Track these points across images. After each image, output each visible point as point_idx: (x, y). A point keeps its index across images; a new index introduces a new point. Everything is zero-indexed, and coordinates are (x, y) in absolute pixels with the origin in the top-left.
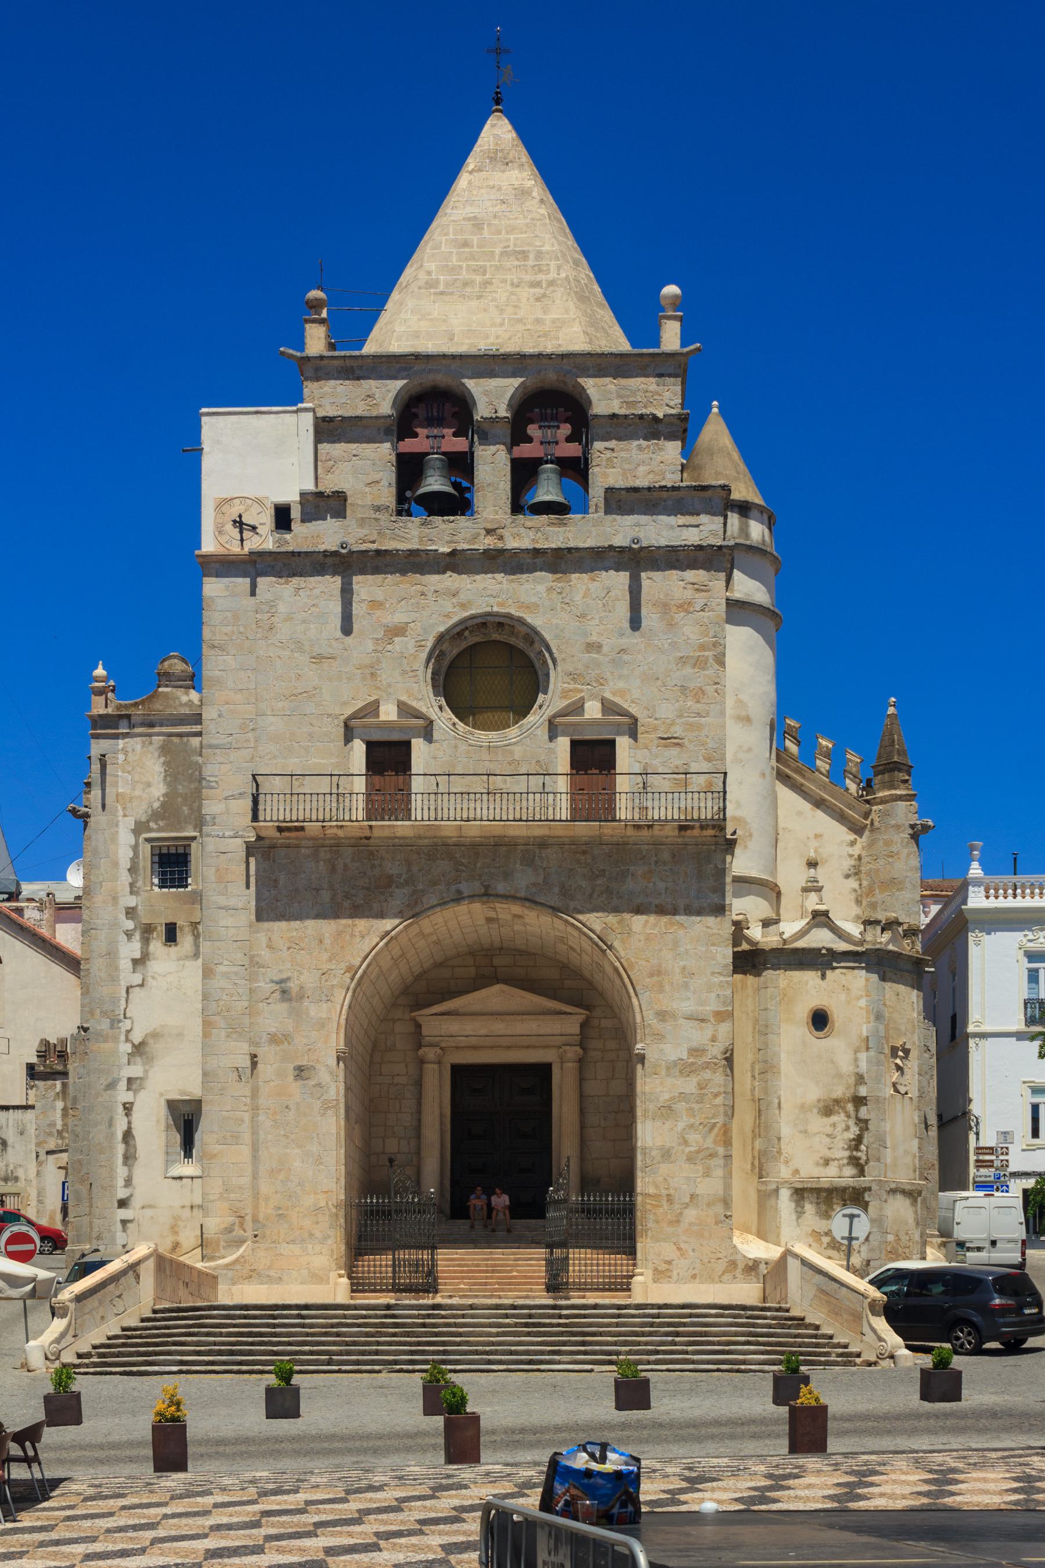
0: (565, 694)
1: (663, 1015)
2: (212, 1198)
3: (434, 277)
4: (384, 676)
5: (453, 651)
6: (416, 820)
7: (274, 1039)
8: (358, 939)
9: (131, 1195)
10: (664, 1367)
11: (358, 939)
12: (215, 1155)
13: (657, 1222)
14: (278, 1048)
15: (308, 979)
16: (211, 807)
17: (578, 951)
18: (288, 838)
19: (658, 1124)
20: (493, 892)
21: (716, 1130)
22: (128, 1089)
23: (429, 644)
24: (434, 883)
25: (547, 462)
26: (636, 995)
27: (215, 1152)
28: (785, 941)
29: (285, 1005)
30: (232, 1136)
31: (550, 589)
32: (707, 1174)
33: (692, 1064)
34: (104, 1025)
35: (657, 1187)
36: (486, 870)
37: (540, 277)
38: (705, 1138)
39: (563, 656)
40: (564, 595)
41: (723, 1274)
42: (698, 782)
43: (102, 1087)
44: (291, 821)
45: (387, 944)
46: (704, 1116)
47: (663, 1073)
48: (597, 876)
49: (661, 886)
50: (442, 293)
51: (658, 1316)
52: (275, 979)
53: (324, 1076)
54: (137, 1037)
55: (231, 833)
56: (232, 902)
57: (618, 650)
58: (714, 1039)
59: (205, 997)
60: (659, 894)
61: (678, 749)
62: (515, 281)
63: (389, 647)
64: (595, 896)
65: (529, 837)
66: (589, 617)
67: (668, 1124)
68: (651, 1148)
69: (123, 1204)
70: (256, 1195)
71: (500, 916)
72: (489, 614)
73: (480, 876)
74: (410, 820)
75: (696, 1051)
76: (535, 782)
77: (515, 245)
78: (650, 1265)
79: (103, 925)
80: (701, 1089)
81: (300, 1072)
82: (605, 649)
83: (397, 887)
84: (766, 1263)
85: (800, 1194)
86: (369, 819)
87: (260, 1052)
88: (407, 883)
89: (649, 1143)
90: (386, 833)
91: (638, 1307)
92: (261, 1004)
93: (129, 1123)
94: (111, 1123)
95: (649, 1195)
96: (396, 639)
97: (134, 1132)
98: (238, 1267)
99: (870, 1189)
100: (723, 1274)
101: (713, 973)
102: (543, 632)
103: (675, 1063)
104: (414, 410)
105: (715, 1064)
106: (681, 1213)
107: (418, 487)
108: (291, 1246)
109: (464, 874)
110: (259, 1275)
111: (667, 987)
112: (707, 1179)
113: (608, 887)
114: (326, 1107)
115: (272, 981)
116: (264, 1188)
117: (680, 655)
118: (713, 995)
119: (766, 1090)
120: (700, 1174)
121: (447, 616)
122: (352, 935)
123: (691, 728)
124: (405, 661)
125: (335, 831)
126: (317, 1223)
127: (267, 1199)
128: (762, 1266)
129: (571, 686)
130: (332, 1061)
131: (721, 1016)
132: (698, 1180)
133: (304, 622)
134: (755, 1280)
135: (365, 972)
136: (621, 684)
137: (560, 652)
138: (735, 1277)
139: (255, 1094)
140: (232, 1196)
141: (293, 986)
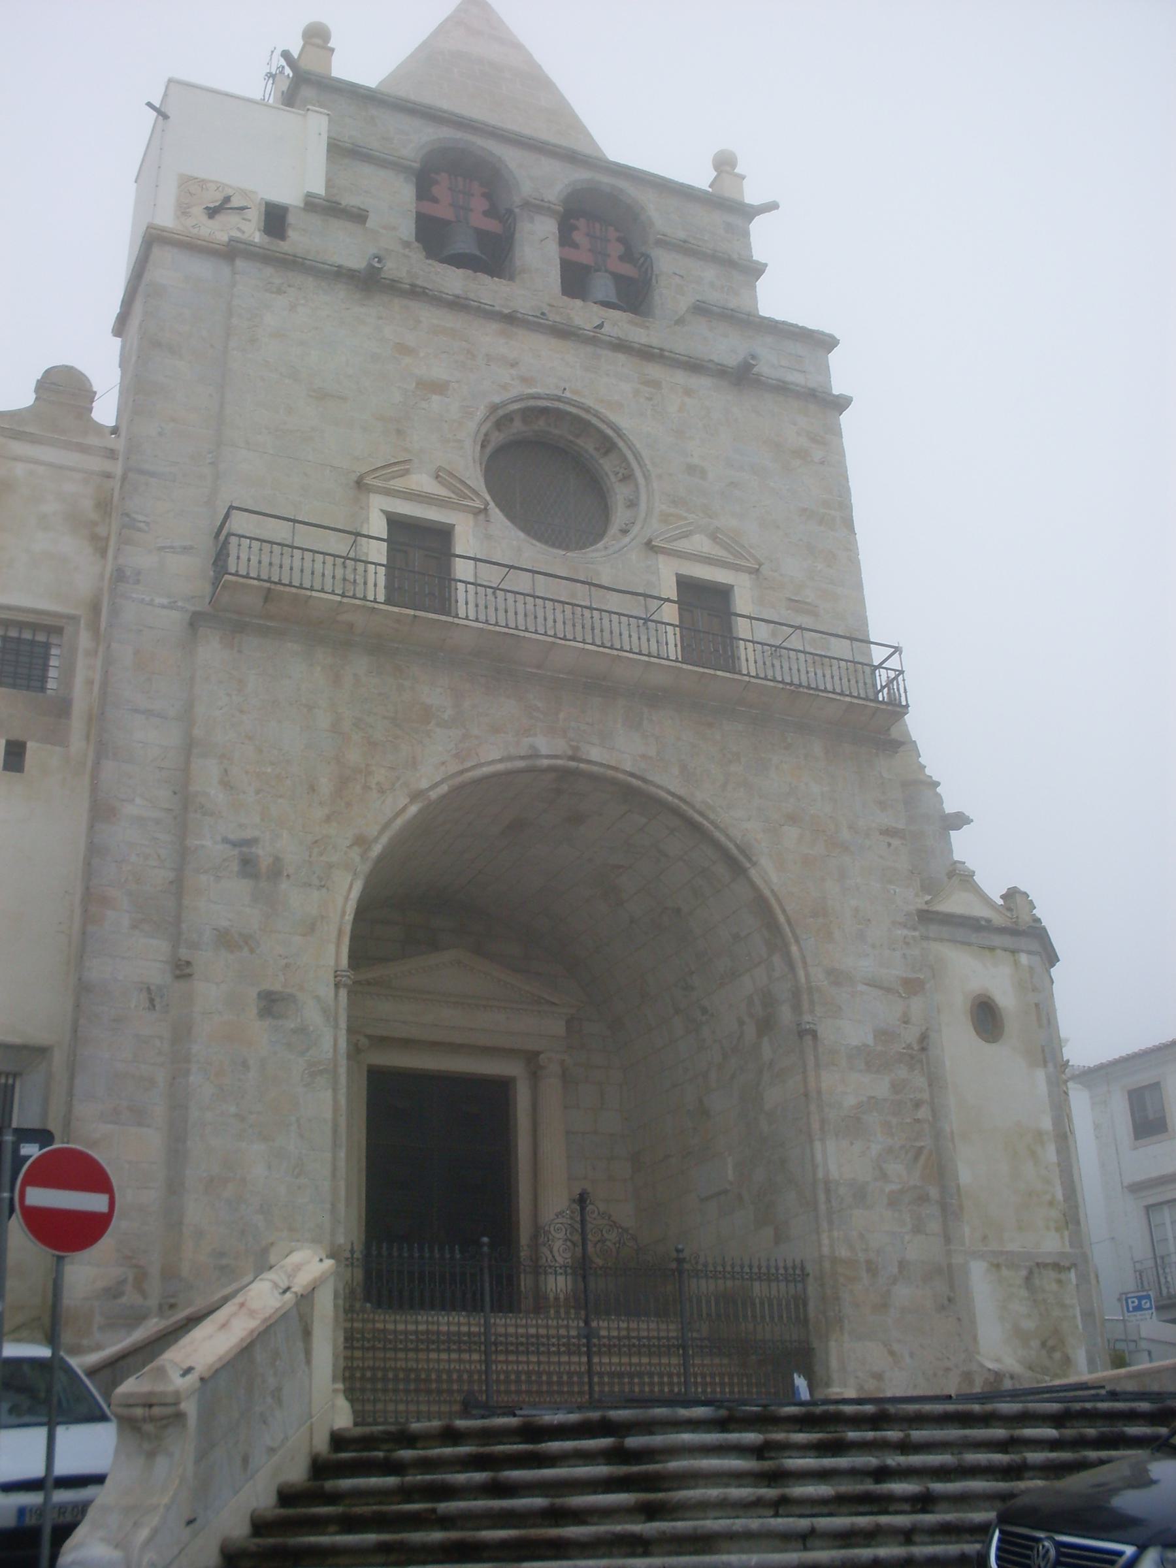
1: (837, 977)
5: (498, 438)
7: (226, 940)
21: (923, 1158)
26: (797, 941)
32: (918, 1229)
52: (232, 837)
55: (165, 601)
58: (906, 1021)
72: (559, 399)
75: (884, 1035)
89: (834, 1173)
96: (435, 398)
115: (225, 840)
121: (505, 387)
122: (366, 788)
130: (326, 991)
132: (907, 1238)
139: (182, 1033)
141: (264, 853)
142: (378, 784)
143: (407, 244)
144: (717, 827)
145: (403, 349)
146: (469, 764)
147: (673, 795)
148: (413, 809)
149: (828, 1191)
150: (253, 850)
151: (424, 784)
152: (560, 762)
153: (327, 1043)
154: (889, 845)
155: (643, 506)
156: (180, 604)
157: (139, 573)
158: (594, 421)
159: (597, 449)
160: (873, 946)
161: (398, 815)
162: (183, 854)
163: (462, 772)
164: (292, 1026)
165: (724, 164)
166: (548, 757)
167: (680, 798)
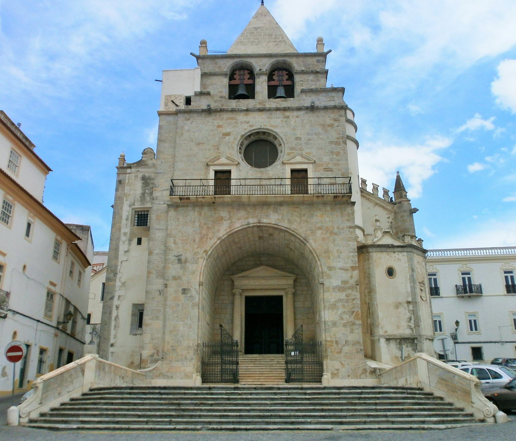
0: (288, 154)
1: (330, 268)
2: (146, 342)
3: (242, 40)
4: (222, 149)
5: (246, 143)
6: (232, 195)
7: (175, 278)
8: (209, 240)
9: (116, 342)
10: (377, 426)
11: (209, 240)
12: (148, 325)
13: (332, 352)
14: (176, 282)
15: (189, 255)
16: (156, 194)
17: (293, 248)
18: (184, 203)
19: (331, 311)
20: (262, 222)
21: (354, 314)
22: (118, 300)
23: (239, 138)
24: (239, 219)
25: (280, 86)
26: (319, 260)
27: (149, 323)
28: (374, 243)
29: (179, 265)
30: (156, 317)
31: (282, 121)
32: (352, 332)
33: (343, 287)
34: (111, 275)
35: (331, 337)
36: (259, 214)
37: (276, 40)
38: (350, 317)
39: (287, 141)
40: (287, 122)
41: (361, 375)
42: (340, 181)
43: (109, 299)
44: (185, 196)
45: (220, 242)
46: (349, 308)
47: (332, 291)
48: (302, 216)
49: (327, 219)
50: (245, 44)
51: (361, 393)
52: (176, 255)
53: (193, 293)
54: (123, 280)
55: (163, 203)
56: (161, 228)
57: (307, 139)
58: (351, 277)
59: (149, 262)
60: (327, 222)
61: (331, 172)
62: (268, 41)
63: (224, 140)
64: (302, 223)
65: (275, 202)
66: (296, 129)
67: (335, 311)
68: (328, 322)
69: (112, 345)
70: (164, 341)
71: (265, 235)
72: (260, 129)
73: (257, 217)
74: (229, 194)
75: (345, 282)
76: (278, 182)
77: (268, 33)
78: (330, 371)
79: (115, 239)
80: (347, 297)
81: (185, 291)
82: (302, 139)
83: (225, 221)
84: (379, 370)
85: (388, 340)
86: (215, 195)
87: (169, 283)
88: (229, 219)
89: (327, 319)
90: (221, 200)
91: (325, 388)
92: (170, 265)
93: (118, 313)
94: (110, 313)
95: (328, 341)
97: (120, 317)
98: (155, 372)
99: (417, 338)
100: (361, 375)
101: (349, 252)
102: (280, 134)
103: (336, 287)
104: (234, 72)
105: (353, 287)
106: (342, 349)
107: (236, 93)
108: (177, 363)
109: (250, 216)
110: (164, 375)
111: (331, 257)
112: (352, 334)
113: (306, 220)
114: (194, 305)
115: (175, 256)
116: (168, 338)
117: (330, 140)
118: (350, 260)
119: (371, 299)
120: (349, 331)
121: (245, 130)
122: (207, 239)
123: (336, 165)
124: (230, 144)
125: (201, 199)
126: (189, 353)
127: (168, 343)
128: (378, 371)
129: (291, 151)
130: (197, 287)
131: (353, 268)
132: (348, 334)
133: (194, 132)
134: (375, 377)
135: (211, 253)
136: (309, 151)
137: (286, 140)
138: (366, 376)
139: (165, 300)
140: (154, 341)
141: (183, 258)
142: (210, 237)
143: (221, 97)
144: (298, 234)
145: (219, 126)
146: (232, 229)
147: (285, 228)
148: (218, 242)
149: (325, 323)
150: (181, 257)
151: (221, 236)
152: (255, 224)
153: (197, 299)
154: (349, 231)
155: (283, 151)
156: (166, 203)
157: (157, 197)
158: (270, 132)
159: (273, 139)
160: (342, 259)
161: (214, 244)
162: (166, 261)
163: (231, 231)
164: (189, 295)
165: (320, 41)
166: (252, 224)
167: (287, 228)
